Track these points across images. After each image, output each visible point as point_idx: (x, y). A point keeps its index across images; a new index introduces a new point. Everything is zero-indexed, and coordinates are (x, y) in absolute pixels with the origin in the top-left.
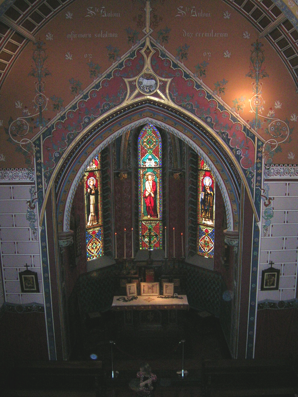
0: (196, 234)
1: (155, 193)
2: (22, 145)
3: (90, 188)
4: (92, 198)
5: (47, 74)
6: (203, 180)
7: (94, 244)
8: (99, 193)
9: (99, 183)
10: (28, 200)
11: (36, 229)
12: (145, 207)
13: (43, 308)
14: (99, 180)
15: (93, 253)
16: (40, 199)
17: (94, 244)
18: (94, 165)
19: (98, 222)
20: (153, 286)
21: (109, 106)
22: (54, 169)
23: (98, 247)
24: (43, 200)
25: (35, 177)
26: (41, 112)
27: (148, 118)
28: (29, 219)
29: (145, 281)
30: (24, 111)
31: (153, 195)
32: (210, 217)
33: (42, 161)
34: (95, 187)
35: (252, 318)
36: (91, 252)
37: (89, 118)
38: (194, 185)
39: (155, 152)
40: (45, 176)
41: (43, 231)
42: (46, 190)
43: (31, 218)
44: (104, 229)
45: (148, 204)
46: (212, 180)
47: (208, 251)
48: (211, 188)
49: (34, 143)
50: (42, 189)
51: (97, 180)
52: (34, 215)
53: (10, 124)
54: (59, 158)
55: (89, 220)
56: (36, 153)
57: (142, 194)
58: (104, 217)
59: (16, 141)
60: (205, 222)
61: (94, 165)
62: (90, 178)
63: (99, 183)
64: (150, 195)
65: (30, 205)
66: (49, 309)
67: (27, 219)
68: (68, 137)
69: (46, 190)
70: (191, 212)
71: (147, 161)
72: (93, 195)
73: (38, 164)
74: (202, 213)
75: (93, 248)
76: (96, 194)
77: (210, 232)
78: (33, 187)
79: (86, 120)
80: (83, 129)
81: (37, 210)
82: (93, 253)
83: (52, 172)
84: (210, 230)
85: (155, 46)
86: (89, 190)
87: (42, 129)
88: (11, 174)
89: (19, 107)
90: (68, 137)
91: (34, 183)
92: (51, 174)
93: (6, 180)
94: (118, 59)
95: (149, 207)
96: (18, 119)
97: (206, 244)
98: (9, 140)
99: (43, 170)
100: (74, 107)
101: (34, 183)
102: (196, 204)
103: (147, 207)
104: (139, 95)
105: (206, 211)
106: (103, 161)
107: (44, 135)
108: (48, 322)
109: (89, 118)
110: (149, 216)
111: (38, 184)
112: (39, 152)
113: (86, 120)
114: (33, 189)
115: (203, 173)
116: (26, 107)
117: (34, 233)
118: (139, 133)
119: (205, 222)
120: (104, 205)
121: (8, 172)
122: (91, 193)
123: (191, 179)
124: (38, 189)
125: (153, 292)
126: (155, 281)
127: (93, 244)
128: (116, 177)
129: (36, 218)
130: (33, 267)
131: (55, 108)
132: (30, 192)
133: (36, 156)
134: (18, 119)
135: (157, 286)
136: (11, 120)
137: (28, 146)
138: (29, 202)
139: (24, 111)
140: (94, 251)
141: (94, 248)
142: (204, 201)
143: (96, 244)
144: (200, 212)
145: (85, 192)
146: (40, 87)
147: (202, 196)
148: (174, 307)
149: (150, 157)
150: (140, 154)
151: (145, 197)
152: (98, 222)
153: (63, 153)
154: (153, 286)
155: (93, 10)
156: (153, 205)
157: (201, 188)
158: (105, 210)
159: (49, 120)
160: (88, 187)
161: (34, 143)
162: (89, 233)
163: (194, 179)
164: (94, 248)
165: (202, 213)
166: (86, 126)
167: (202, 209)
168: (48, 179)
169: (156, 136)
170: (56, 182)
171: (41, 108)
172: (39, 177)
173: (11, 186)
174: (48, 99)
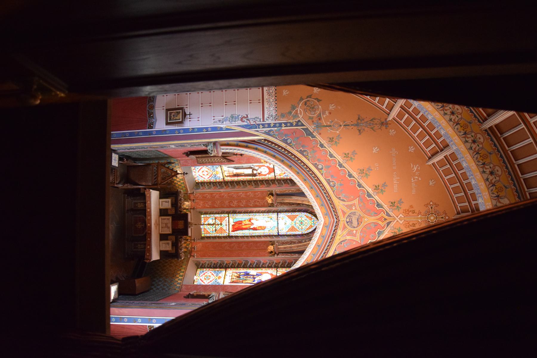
1: (255, 229)
2: (297, 111)
4: (249, 171)
5: (359, 131)
6: (267, 273)
9: (263, 177)
10: (249, 116)
11: (223, 122)
12: (241, 220)
13: (152, 128)
14: (265, 177)
16: (250, 127)
19: (228, 176)
20: (168, 228)
21: (333, 187)
22: (276, 138)
23: (204, 176)
24: (249, 129)
25: (269, 121)
26: (327, 126)
27: (323, 221)
28: (232, 117)
29: (173, 220)
30: (327, 112)
31: (252, 227)
33: (283, 128)
34: (259, 174)
35: (140, 320)
37: (322, 168)
39: (293, 229)
40: (270, 131)
41: (221, 129)
42: (257, 131)
43: (233, 118)
44: (221, 182)
45: (244, 222)
49: (299, 121)
50: (259, 128)
51: (265, 175)
52: (235, 121)
53: (315, 99)
54: (286, 143)
56: (290, 123)
57: (253, 217)
58: (232, 182)
59: (300, 105)
63: (263, 177)
64: (252, 224)
65: (244, 117)
66: (150, 133)
67: (232, 115)
68: (305, 151)
69: (257, 131)
71: (284, 221)
73: (280, 124)
74: (237, 273)
75: (203, 172)
77: (219, 281)
78: (260, 120)
79: (320, 167)
80: (312, 164)
81: (240, 123)
83: (273, 137)
84: (221, 281)
85: (387, 226)
86: (256, 168)
87: (311, 128)
88: (271, 100)
89: (331, 108)
90: (305, 151)
91: (263, 121)
92: (272, 136)
93: (266, 96)
94: (375, 193)
95: (241, 223)
96: (320, 107)
97: (208, 278)
98: (302, 99)
99: (276, 129)
100: (331, 156)
101: (263, 121)
102: (245, 267)
103: (241, 221)
104: (344, 213)
105: (239, 277)
107: (306, 130)
108: (138, 132)
109: (322, 168)
110: (233, 224)
111: (263, 125)
112: (292, 125)
113: (320, 167)
114: (258, 120)
116: (330, 113)
117: (219, 121)
118: (309, 213)
120: (243, 182)
121: (273, 98)
122: (253, 169)
124: (259, 125)
125: (162, 228)
126: (173, 229)
128: (269, 193)
129: (233, 122)
130: (189, 120)
131: (330, 139)
132: (256, 118)
133: (287, 123)
134: (320, 107)
135: (169, 231)
136: (319, 100)
137: (296, 115)
138: (247, 117)
139: (327, 112)
140: (200, 173)
142: (247, 274)
144: (237, 271)
146: (348, 125)
147: (253, 272)
148: (148, 247)
149: (288, 224)
150: (290, 214)
151: (250, 220)
152: (228, 176)
153: (291, 146)
154: (168, 228)
155: (417, 170)
156: (244, 227)
158: (238, 183)
159: (320, 134)
161: (299, 121)
165: (237, 273)
166: (315, 166)
167: (240, 273)
168: (268, 133)
169: (308, 229)
170: (265, 140)
171: (330, 126)
172: (269, 125)
173: (261, 101)
174: (338, 132)
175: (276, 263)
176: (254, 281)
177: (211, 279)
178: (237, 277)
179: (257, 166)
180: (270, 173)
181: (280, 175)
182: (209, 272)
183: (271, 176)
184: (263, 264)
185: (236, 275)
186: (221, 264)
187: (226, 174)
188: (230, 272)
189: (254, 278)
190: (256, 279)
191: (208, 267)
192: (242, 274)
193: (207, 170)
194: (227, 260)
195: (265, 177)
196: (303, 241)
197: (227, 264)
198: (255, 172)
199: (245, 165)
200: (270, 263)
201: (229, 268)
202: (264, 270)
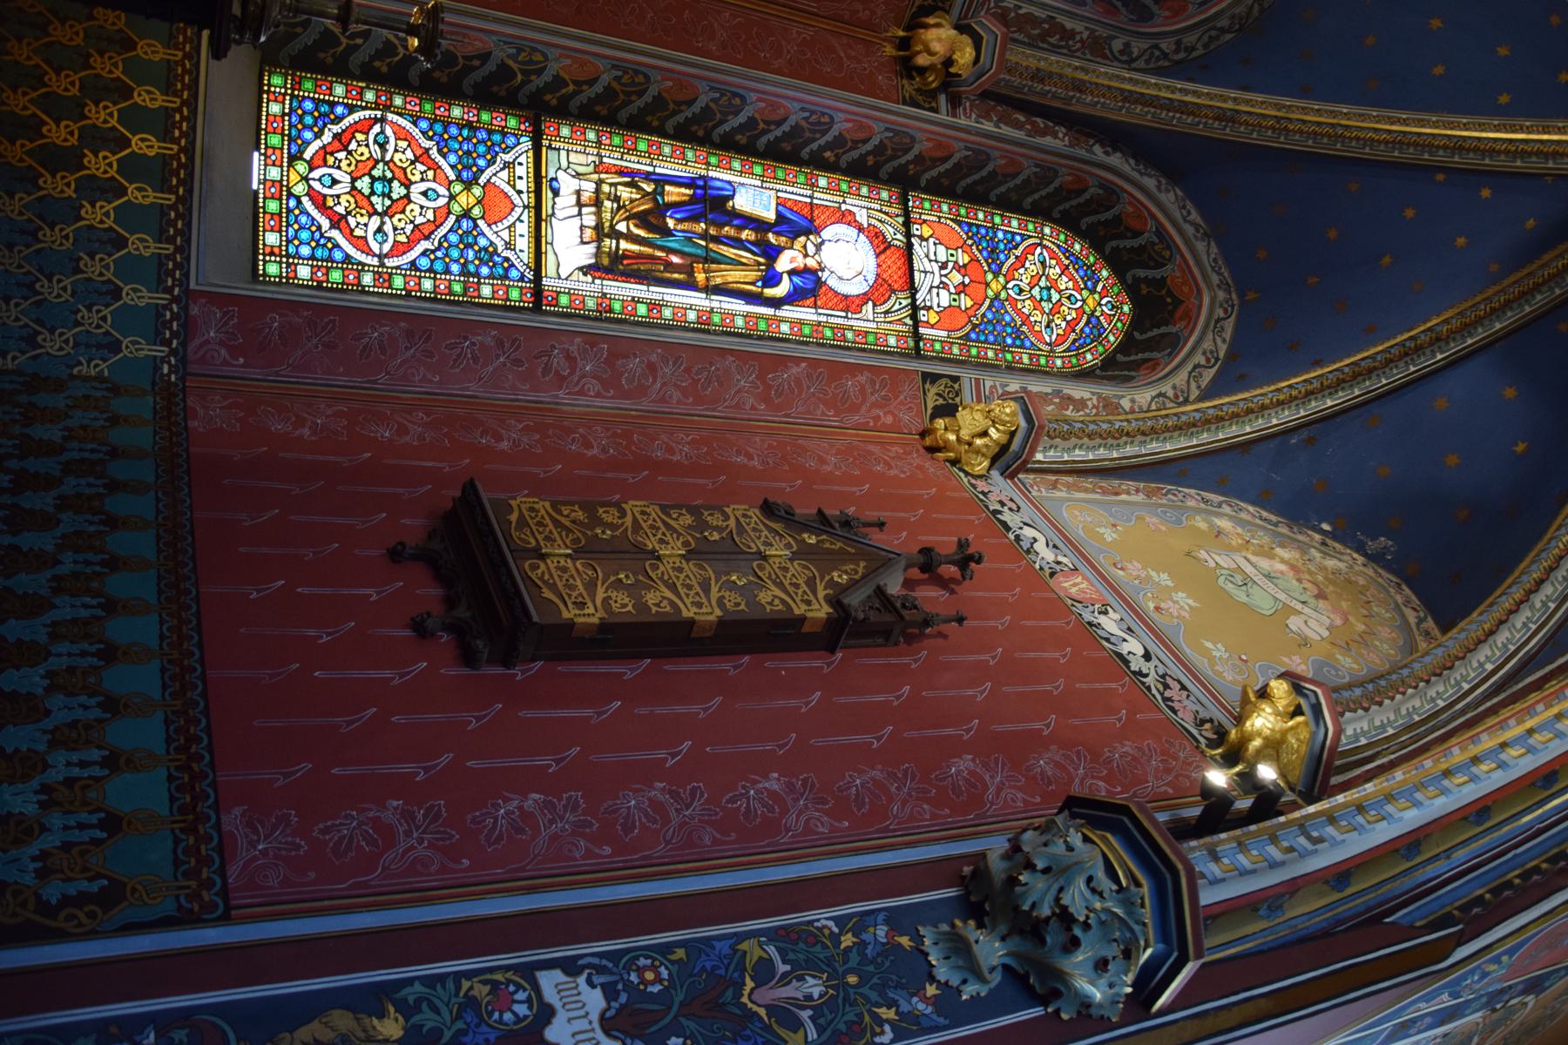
0: (448, 91)
6: (847, 218)
32: (616, 257)
38: (822, 149)
46: (865, 298)
47: (320, 202)
48: (810, 286)
60: (566, 201)
70: (653, 90)
74: (633, 178)
97: (384, 188)
102: (696, 132)
105: (652, 219)
115: (889, 232)
119: (566, 201)
123: (875, 141)
142: (711, 204)
144: (632, 163)
147: (755, 196)
157: (797, 193)
163: (863, 157)
165: (633, 178)
167: (661, 181)
175: (919, 159)
176: (772, 279)
177: (419, 210)
178: (642, 219)
182: (398, 132)
184: (840, 141)
185: (625, 194)
186: (504, 72)
188: (575, 161)
189: (772, 253)
190: (783, 263)
191: (371, 76)
192: (673, 193)
194: (566, 47)
196: (1117, 45)
197: (558, 82)
200: (880, 149)
201: (563, 112)
202: (823, 191)
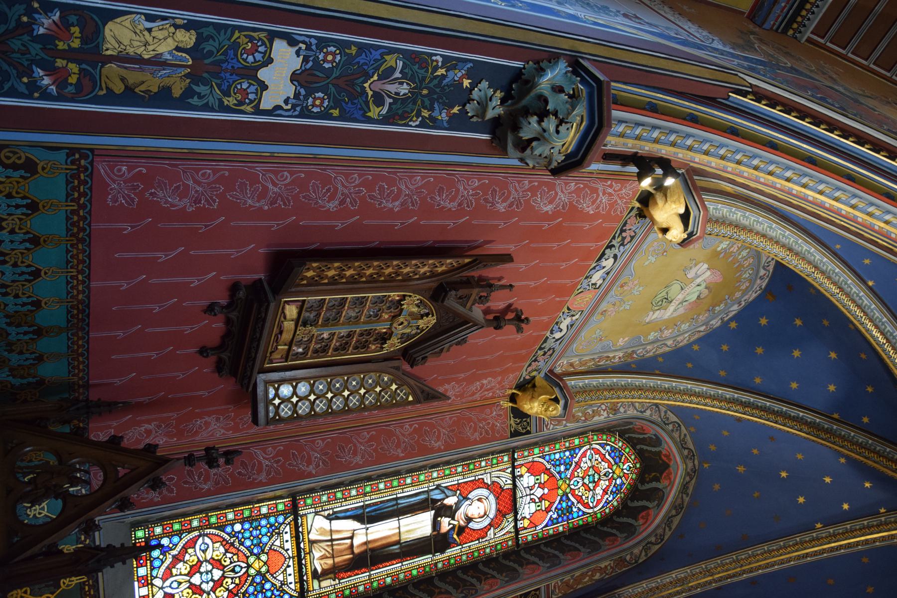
3: (458, 505)
4: (419, 526)
7: (217, 574)
8: (439, 556)
14: (484, 543)
15: (168, 574)
17: (217, 574)
18: (533, 507)
34: (461, 530)
36: (177, 559)
51: (484, 532)
55: (337, 524)
61: (533, 507)
62: (492, 498)
63: (474, 545)
72: (436, 525)
75: (195, 569)
76: (438, 542)
82: (168, 574)
86: (451, 501)
106: (546, 544)
122: (443, 511)
127: (217, 563)
141: (196, 579)
143: (218, 584)
145: (446, 483)
160: (463, 492)
162: (275, 531)
164: (196, 579)
179: (453, 489)
180: (501, 513)
181: (533, 524)
183: (501, 535)
187: (318, 560)
193: (217, 551)
195: (484, 543)
198: (445, 524)
199: (409, 490)
